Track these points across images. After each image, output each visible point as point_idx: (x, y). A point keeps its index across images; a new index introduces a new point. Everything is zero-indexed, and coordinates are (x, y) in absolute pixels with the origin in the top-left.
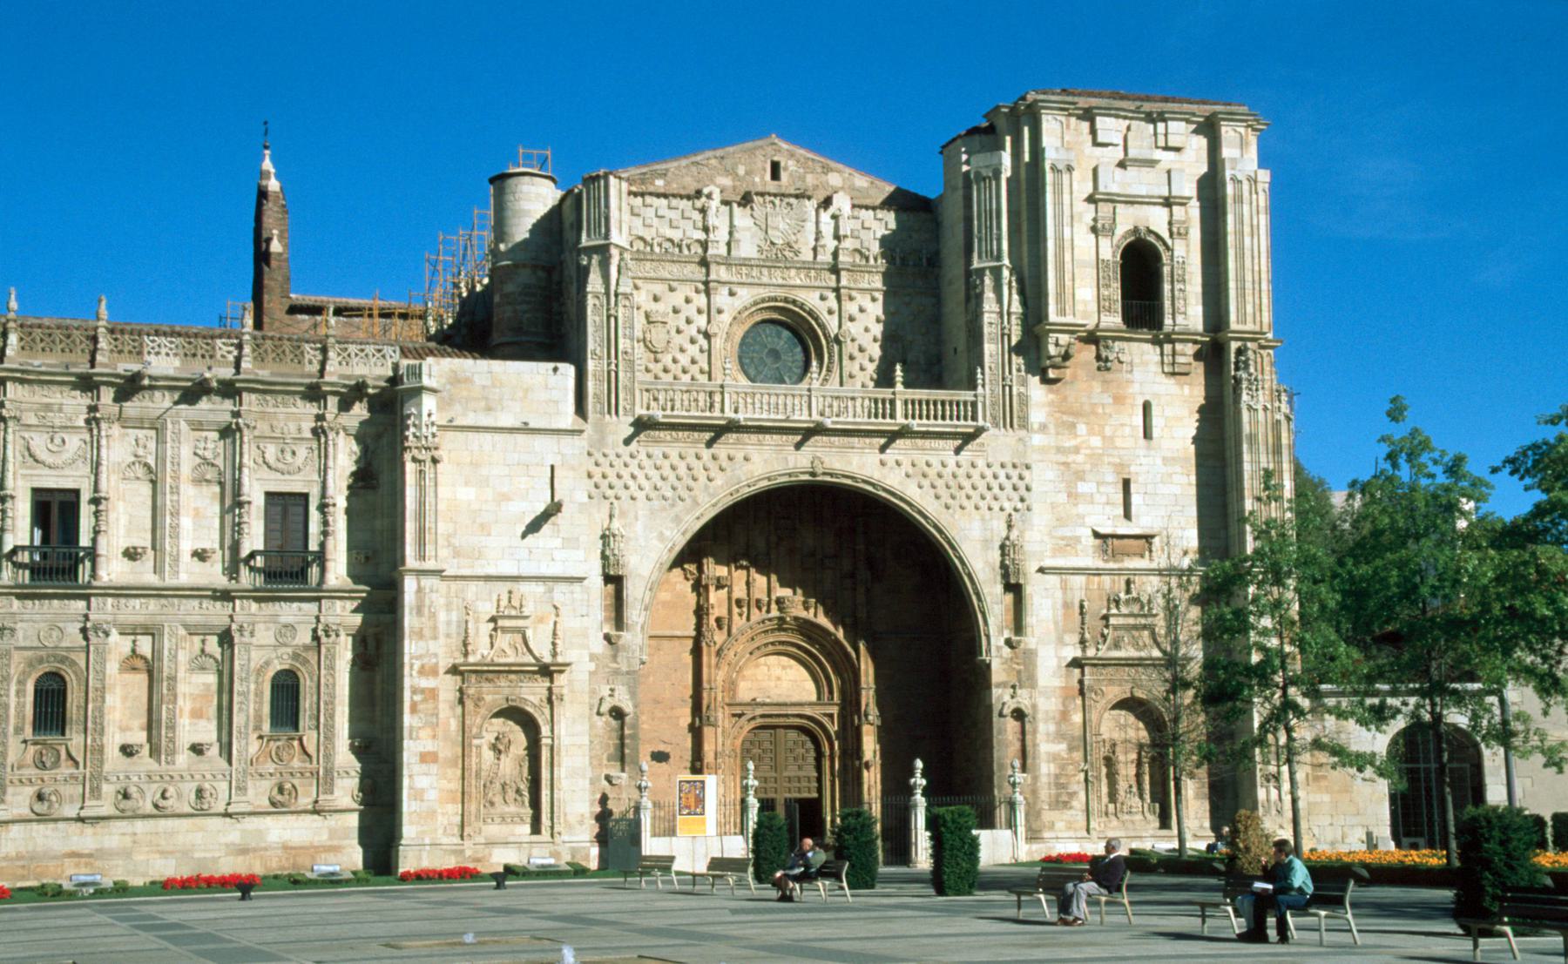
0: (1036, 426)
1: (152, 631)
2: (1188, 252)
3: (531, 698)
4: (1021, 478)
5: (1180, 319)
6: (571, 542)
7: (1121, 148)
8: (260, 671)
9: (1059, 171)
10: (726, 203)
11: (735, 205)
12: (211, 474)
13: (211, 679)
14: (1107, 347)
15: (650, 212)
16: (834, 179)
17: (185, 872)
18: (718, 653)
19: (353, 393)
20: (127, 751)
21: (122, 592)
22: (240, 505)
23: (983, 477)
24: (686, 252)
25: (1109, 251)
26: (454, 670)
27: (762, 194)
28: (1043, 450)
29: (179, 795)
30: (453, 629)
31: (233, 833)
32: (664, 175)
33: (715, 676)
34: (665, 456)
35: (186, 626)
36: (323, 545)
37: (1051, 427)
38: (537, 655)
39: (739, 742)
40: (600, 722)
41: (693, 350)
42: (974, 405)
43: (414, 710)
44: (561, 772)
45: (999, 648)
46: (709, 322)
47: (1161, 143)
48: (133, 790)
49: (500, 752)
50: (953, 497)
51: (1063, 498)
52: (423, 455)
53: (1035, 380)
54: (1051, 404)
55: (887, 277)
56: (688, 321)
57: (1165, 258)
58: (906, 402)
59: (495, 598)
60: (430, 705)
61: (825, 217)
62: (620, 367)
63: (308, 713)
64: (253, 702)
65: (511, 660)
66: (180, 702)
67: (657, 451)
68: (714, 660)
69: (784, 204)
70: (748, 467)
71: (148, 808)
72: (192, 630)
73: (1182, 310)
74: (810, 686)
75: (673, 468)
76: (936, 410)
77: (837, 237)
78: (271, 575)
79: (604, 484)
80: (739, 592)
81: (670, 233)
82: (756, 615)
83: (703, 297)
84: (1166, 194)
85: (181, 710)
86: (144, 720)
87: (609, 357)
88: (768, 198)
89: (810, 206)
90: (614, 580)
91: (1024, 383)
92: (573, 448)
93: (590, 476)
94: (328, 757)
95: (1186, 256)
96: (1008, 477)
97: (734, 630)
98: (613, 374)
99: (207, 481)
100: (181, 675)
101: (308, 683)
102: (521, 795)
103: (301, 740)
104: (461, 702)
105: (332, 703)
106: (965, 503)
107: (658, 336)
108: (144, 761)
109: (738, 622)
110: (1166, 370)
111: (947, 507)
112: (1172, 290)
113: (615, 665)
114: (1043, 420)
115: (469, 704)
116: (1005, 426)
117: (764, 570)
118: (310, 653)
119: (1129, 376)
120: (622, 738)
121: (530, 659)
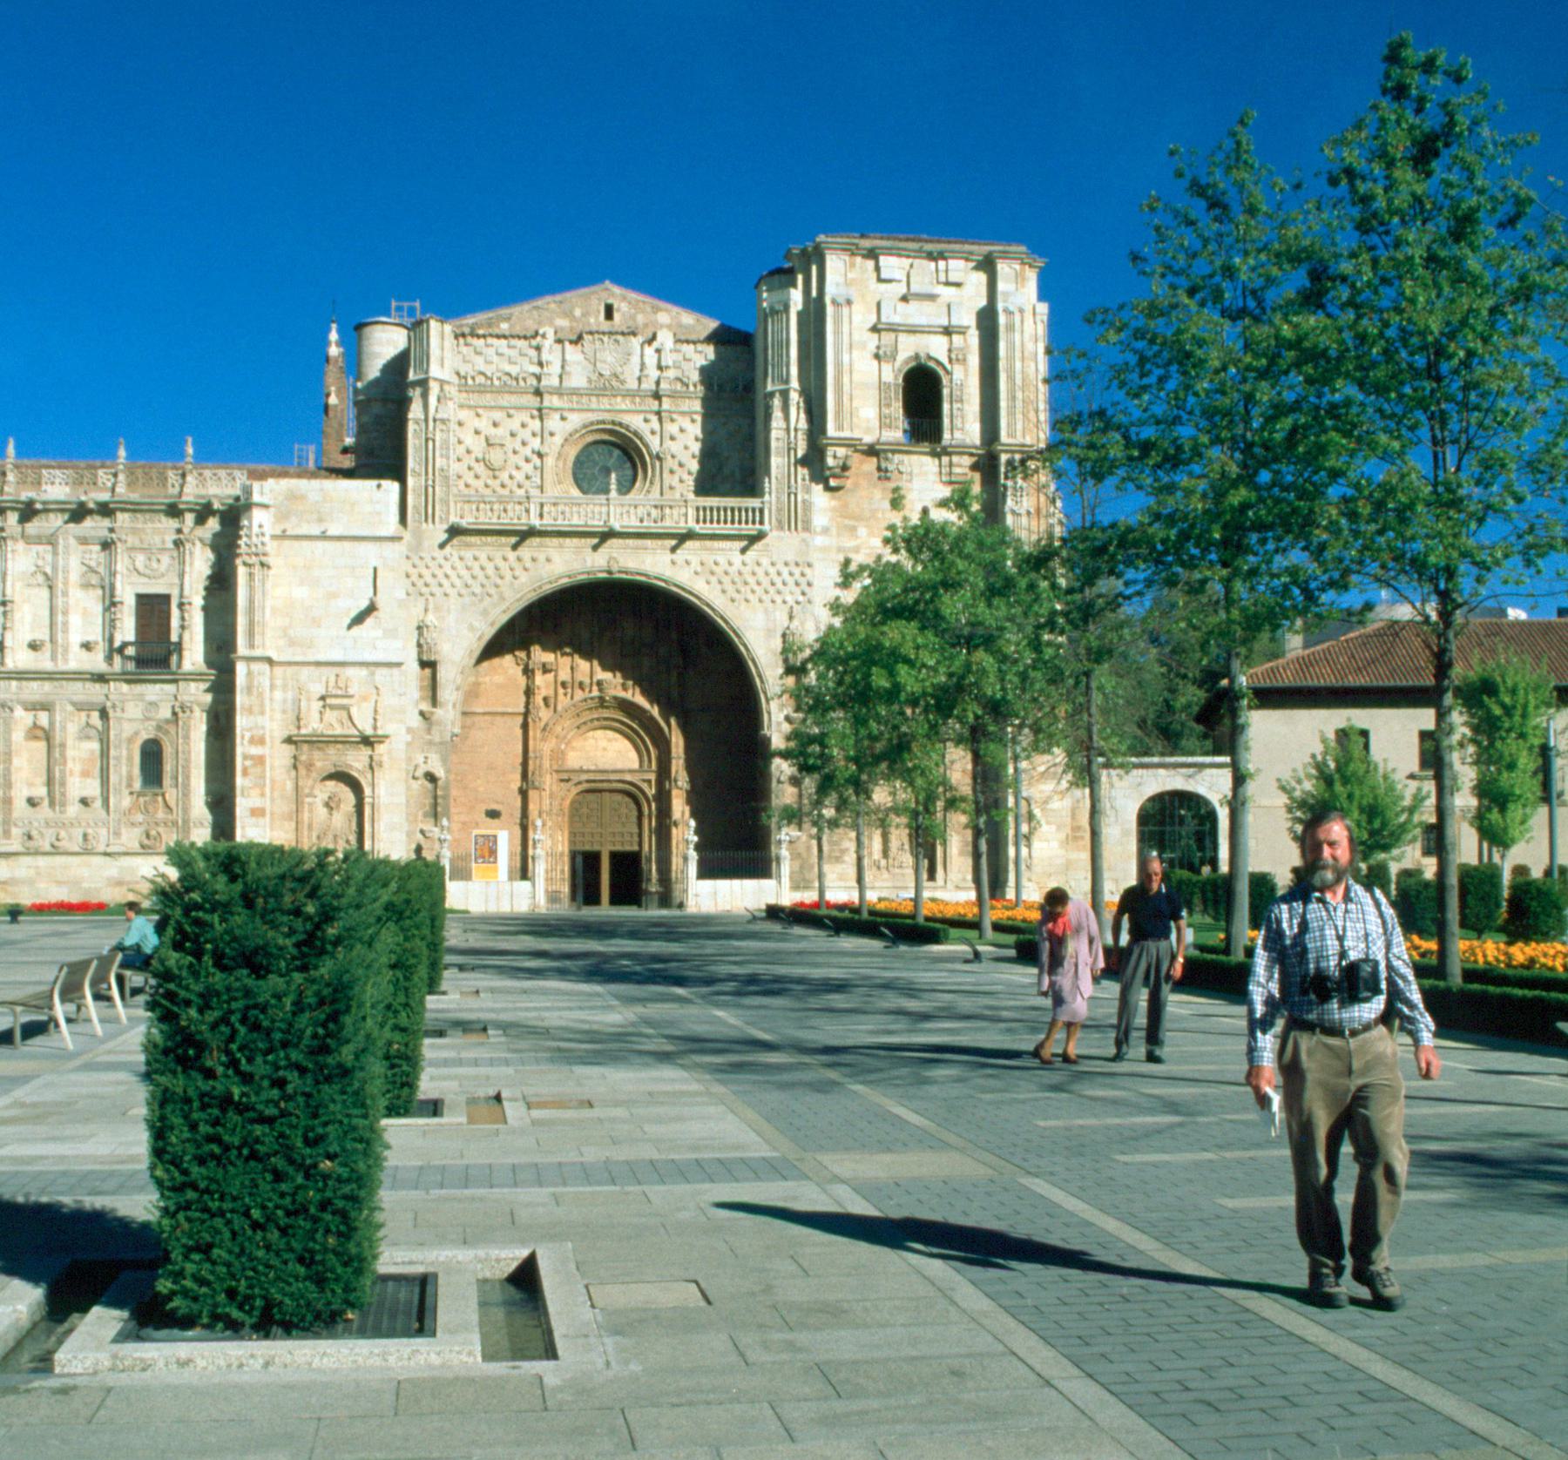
0: (818, 529)
1: (46, 707)
2: (966, 376)
3: (356, 765)
4: (803, 575)
5: (957, 435)
6: (391, 633)
7: (904, 283)
8: (130, 740)
10: (559, 341)
12: (94, 580)
13: (95, 746)
14: (887, 459)
15: (491, 351)
16: (663, 318)
17: (75, 899)
18: (544, 729)
19: (203, 513)
20: (32, 802)
21: (22, 676)
22: (114, 604)
23: (767, 574)
24: (522, 383)
26: (289, 740)
27: (591, 333)
28: (824, 549)
29: (70, 838)
30: (289, 705)
31: (112, 868)
32: (508, 319)
33: (543, 747)
35: (74, 704)
36: (181, 637)
37: (834, 531)
39: (568, 802)
40: (416, 785)
41: (528, 468)
42: (761, 511)
43: (245, 772)
44: (381, 826)
45: (779, 724)
47: (942, 278)
48: (34, 833)
50: (738, 591)
52: (254, 560)
53: (818, 489)
54: (833, 509)
55: (706, 402)
56: (524, 444)
57: (945, 381)
58: (698, 509)
60: (258, 770)
64: (128, 765)
65: (338, 731)
66: (70, 764)
67: (468, 554)
68: (539, 735)
70: (549, 567)
71: (48, 848)
72: (79, 707)
74: (633, 755)
75: (482, 568)
77: (660, 368)
78: (141, 661)
80: (564, 675)
81: (508, 368)
82: (579, 695)
83: (537, 422)
84: (946, 323)
86: (44, 778)
89: (635, 342)
91: (808, 491)
92: (399, 549)
93: (408, 576)
94: (186, 810)
97: (559, 708)
100: (70, 743)
103: (163, 795)
106: (750, 596)
107: (496, 457)
108: (45, 810)
109: (563, 701)
111: (733, 600)
115: (302, 771)
117: (587, 655)
120: (435, 797)
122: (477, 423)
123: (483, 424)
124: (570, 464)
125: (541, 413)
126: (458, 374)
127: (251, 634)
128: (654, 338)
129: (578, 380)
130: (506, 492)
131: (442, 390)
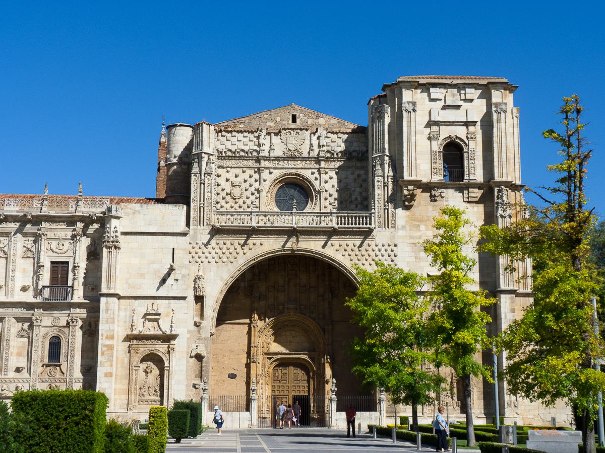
0: (400, 227)
2: (476, 146)
3: (160, 349)
4: (392, 251)
5: (472, 177)
7: (443, 101)
8: (44, 337)
9: (409, 112)
10: (269, 134)
11: (273, 134)
12: (30, 254)
13: (26, 340)
15: (235, 139)
16: (321, 121)
18: (259, 331)
22: (39, 267)
25: (437, 146)
27: (285, 129)
36: (73, 284)
37: (408, 228)
41: (253, 198)
43: (103, 354)
44: (173, 382)
46: (260, 185)
49: (148, 373)
51: (413, 259)
52: (111, 244)
54: (408, 216)
59: (146, 305)
60: (110, 352)
61: (314, 138)
62: (205, 205)
63: (63, 355)
64: (42, 350)
66: (11, 349)
67: (221, 242)
69: (295, 132)
73: (473, 172)
76: (363, 221)
79: (196, 256)
85: (12, 353)
87: (200, 201)
88: (288, 131)
90: (199, 299)
95: (475, 148)
96: (386, 251)
98: (202, 208)
99: (29, 257)
100: (12, 338)
101: (64, 342)
102: (156, 392)
104: (129, 352)
105: (74, 350)
107: (237, 192)
110: (465, 200)
113: (199, 335)
114: (404, 224)
115: (132, 351)
116: (385, 227)
118: (66, 329)
119: (447, 203)
120: (201, 367)
121: (159, 333)
122: (228, 176)
123: (231, 175)
124: (274, 195)
125: (259, 171)
126: (218, 150)
129: (278, 153)
130: (241, 210)
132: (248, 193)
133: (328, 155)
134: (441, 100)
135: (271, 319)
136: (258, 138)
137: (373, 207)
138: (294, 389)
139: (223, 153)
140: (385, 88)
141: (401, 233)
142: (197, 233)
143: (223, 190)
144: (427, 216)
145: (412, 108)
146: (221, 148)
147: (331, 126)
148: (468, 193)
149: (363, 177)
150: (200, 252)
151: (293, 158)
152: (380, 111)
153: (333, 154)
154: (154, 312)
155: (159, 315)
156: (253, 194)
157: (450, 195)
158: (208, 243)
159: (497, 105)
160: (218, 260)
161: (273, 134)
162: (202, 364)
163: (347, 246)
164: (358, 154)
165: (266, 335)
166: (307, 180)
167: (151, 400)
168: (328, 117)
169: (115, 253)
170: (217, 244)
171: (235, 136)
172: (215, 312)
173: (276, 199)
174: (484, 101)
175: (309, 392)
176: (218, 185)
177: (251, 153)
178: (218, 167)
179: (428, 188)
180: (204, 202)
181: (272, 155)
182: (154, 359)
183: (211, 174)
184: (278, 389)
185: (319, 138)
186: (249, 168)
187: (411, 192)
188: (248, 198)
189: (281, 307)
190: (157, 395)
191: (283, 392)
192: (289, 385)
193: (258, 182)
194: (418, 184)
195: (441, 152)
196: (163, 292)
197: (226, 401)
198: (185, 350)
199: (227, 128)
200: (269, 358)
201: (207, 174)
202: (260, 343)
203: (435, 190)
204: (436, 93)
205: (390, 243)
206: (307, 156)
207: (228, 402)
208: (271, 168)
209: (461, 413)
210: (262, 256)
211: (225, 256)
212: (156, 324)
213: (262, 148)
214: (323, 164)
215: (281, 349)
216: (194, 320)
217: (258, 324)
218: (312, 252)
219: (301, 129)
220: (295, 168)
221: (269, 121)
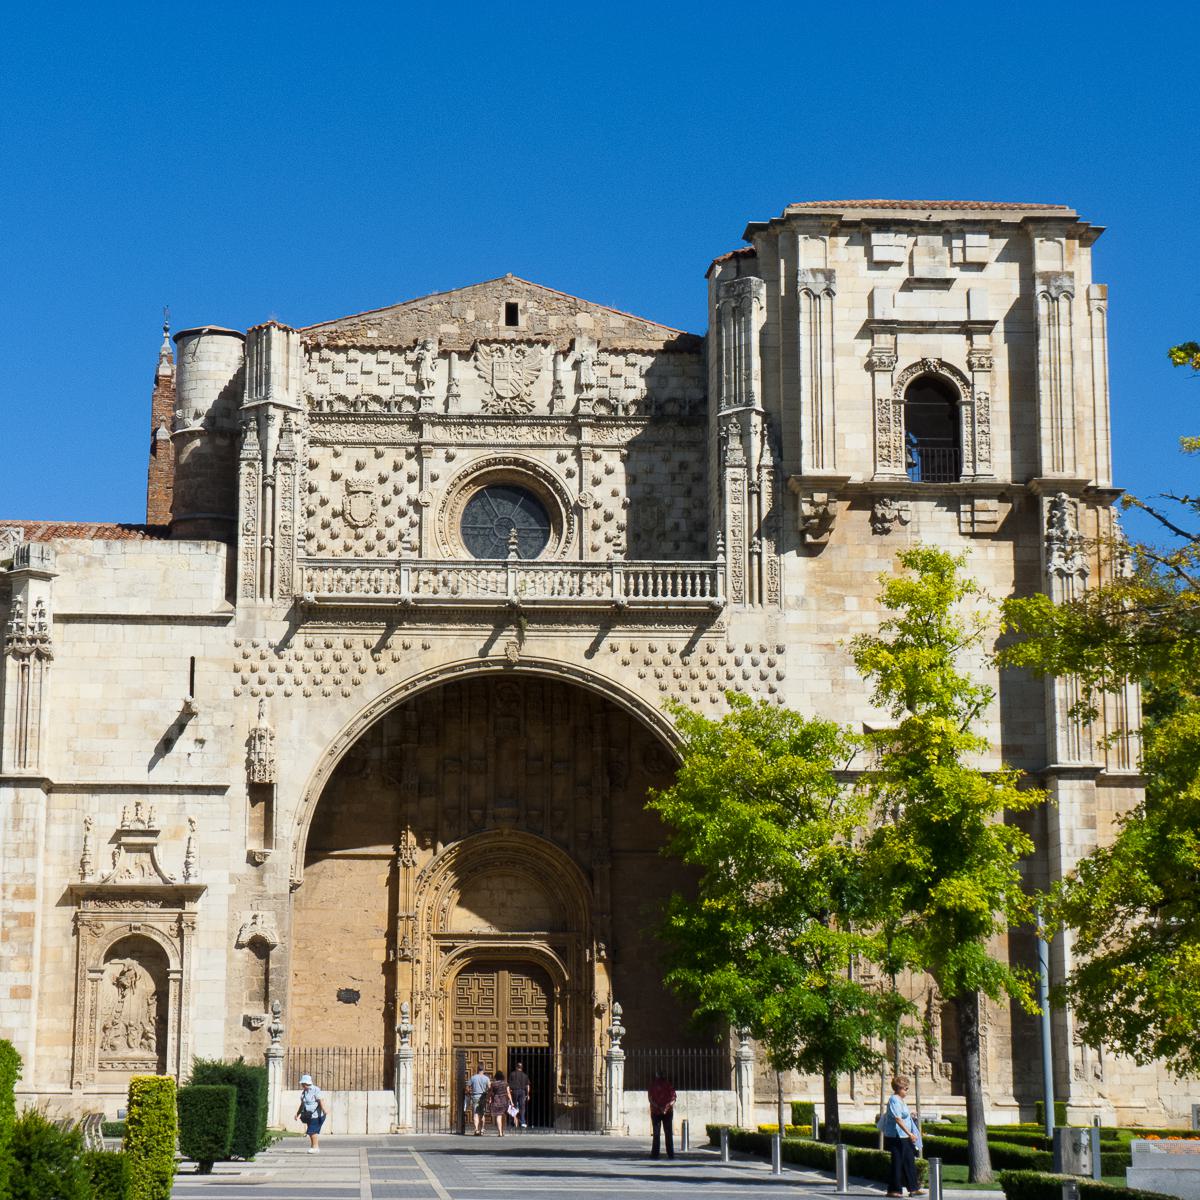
0: (791, 601)
2: (992, 387)
3: (159, 926)
4: (771, 665)
5: (982, 468)
7: (905, 267)
9: (817, 297)
10: (445, 354)
11: (455, 356)
15: (355, 368)
16: (583, 320)
27: (487, 342)
30: (71, 846)
34: (347, 647)
37: (812, 602)
38: (167, 876)
44: (190, 1012)
46: (421, 489)
49: (124, 987)
54: (813, 573)
60: (23, 932)
61: (565, 365)
62: (277, 543)
67: (319, 640)
69: (515, 350)
73: (986, 456)
76: (693, 584)
79: (253, 679)
81: (377, 390)
84: (964, 318)
87: (263, 533)
88: (495, 346)
90: (261, 793)
95: (992, 391)
96: (755, 664)
98: (268, 552)
102: (148, 1038)
104: (76, 932)
107: (360, 508)
110: (963, 530)
112: (973, 434)
113: (261, 888)
115: (84, 931)
116: (751, 602)
119: (915, 538)
120: (267, 973)
121: (155, 881)
122: (337, 465)
123: (344, 465)
124: (458, 518)
125: (418, 453)
126: (310, 398)
127: (22, 746)
128: (572, 347)
130: (372, 556)
131: (286, 420)
132: (390, 512)
133: (603, 411)
134: (899, 264)
135: (451, 845)
136: (417, 364)
137: (721, 549)
138: (513, 1031)
139: (325, 404)
140: (751, 232)
141: (793, 617)
142: (254, 617)
143: (324, 503)
144: (864, 573)
145: (824, 286)
146: (318, 391)
147: (610, 335)
148: (972, 512)
149: (695, 468)
150: (263, 666)
151: (509, 419)
152: (739, 295)
153: (614, 409)
154: (141, 827)
155: (155, 833)
156: (402, 514)
157: (925, 517)
158: (285, 643)
159: (1048, 278)
160: (310, 689)
161: (455, 356)
162: (267, 963)
163: (652, 651)
164: (682, 407)
165: (437, 889)
166: (546, 476)
167: (134, 1060)
168: (601, 309)
169: (38, 671)
170: (309, 646)
171: (356, 361)
172: (304, 827)
173: (464, 529)
174: (1015, 267)
175: (551, 1038)
176: (312, 490)
177: (398, 405)
178: (311, 442)
179: (865, 497)
180: (273, 534)
181: (453, 410)
182: (142, 950)
183: (293, 460)
184: (471, 1031)
185: (576, 365)
186: (393, 444)
187: (821, 509)
188: (389, 524)
189: (477, 814)
190: (149, 1046)
191: (482, 1038)
192: (499, 1020)
193: (416, 483)
194: (838, 488)
195: (899, 402)
196: (163, 774)
197: (331, 1062)
198: (224, 926)
199: (334, 339)
200: (447, 950)
201: (282, 460)
202: (420, 909)
203: (885, 504)
204: (886, 245)
205: (766, 645)
206: (546, 412)
207: (337, 1063)
208: (451, 445)
209: (953, 1094)
210: (427, 678)
211: (328, 680)
212: (146, 857)
213: (426, 393)
214: (587, 435)
215: (480, 926)
216: (249, 848)
217: (415, 858)
218: (559, 668)
219: (530, 343)
220: (514, 446)
221: (444, 322)
